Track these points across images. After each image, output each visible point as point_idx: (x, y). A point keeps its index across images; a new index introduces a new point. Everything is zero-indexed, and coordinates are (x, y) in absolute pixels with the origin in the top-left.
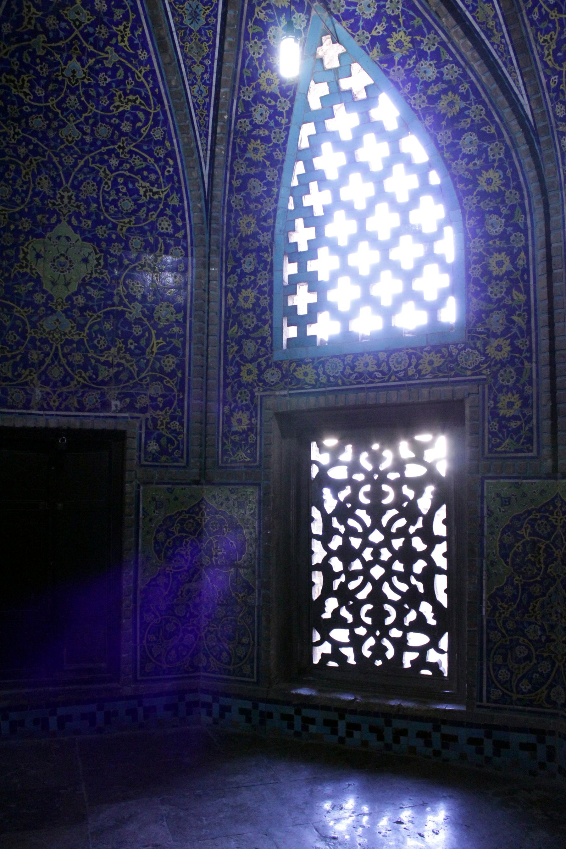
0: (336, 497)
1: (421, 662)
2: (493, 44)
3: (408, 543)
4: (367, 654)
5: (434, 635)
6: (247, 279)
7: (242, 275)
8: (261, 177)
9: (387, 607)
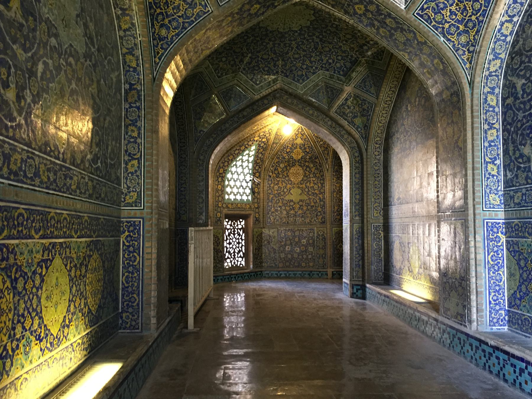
1: (240, 264)
4: (233, 264)
5: (242, 258)
7: (219, 182)
8: (228, 162)
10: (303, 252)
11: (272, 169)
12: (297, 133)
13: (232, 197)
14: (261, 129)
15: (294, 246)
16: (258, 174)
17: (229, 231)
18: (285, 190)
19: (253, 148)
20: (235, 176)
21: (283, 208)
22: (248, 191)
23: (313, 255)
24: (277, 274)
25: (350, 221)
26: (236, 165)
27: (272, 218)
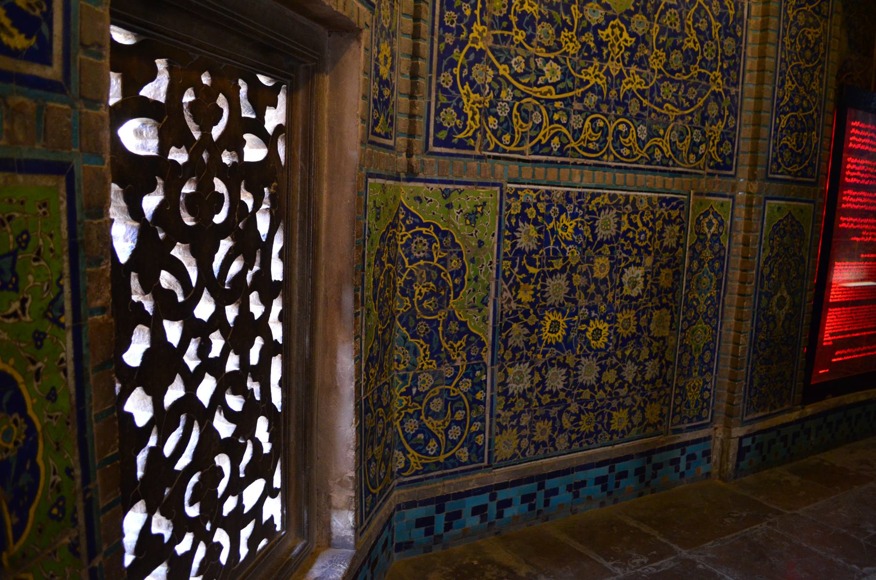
0: (135, 211)
10: (625, 341)
15: (583, 312)
21: (544, 30)
23: (668, 357)
24: (479, 510)
27: (470, 101)
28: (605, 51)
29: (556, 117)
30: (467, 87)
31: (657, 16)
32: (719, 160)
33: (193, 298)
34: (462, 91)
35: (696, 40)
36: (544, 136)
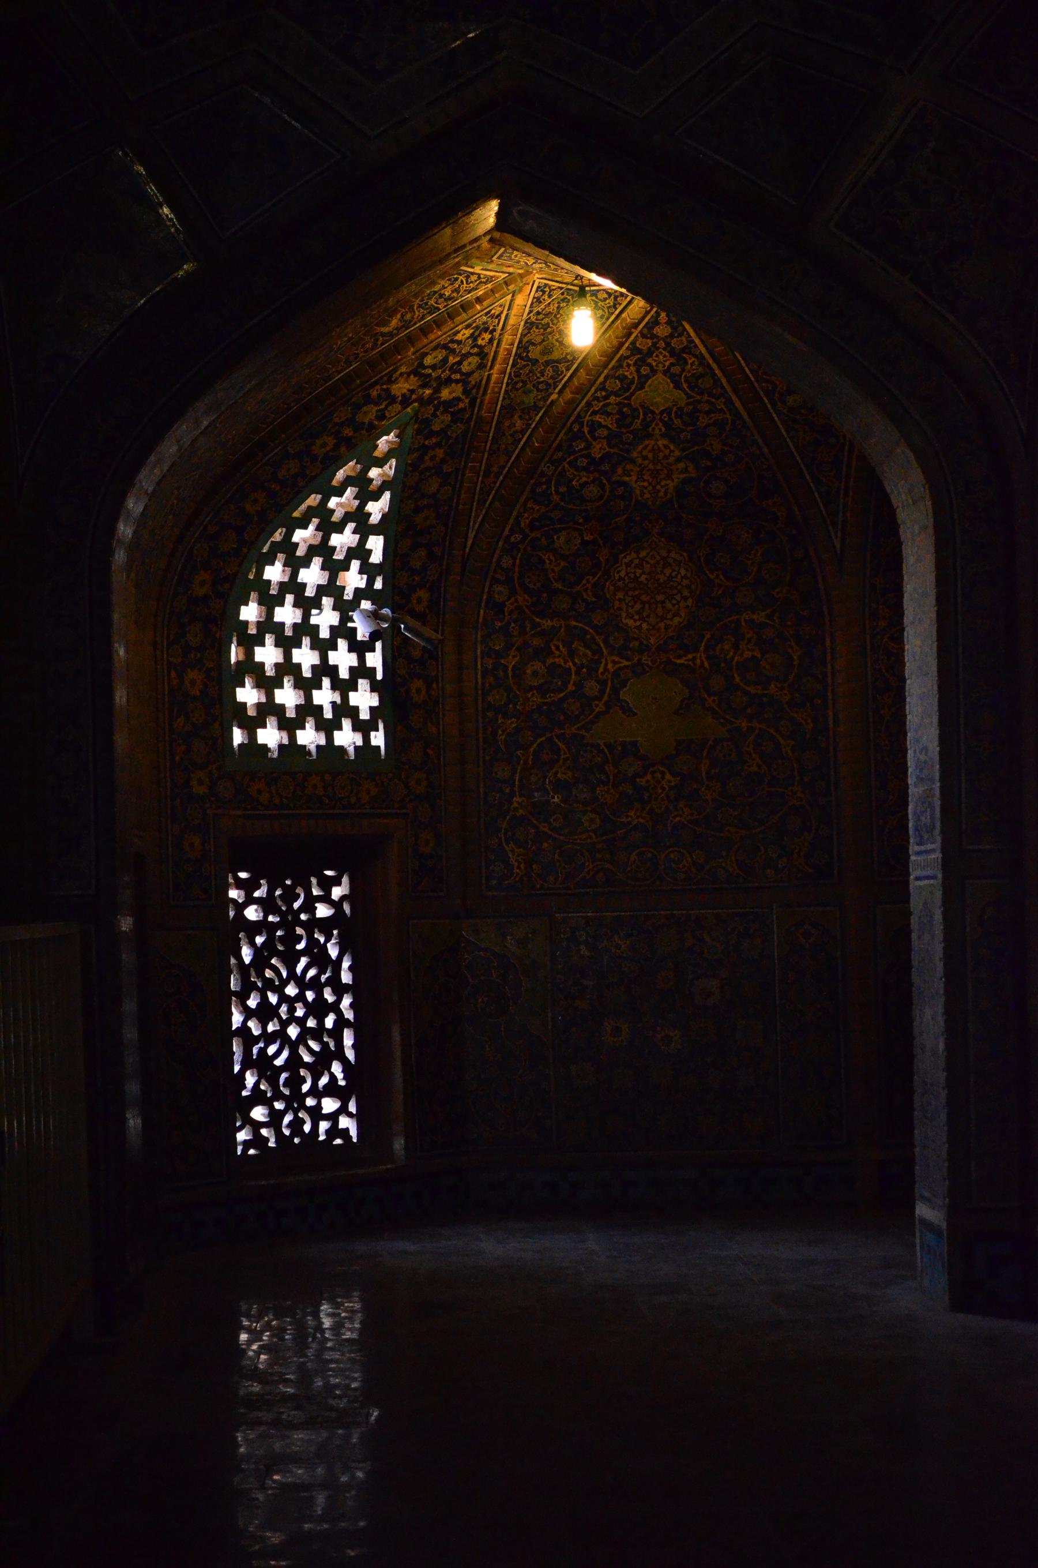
0: (252, 944)
1: (334, 1131)
2: (482, 482)
3: (319, 995)
6: (193, 655)
9: (303, 1072)
11: (506, 562)
12: (645, 344)
13: (270, 736)
14: (425, 331)
16: (423, 594)
17: (259, 940)
18: (591, 687)
19: (384, 443)
20: (287, 614)
22: (364, 699)
25: (946, 864)
26: (288, 547)
28: (646, 796)
29: (599, 856)
30: (511, 844)
31: (705, 753)
32: (810, 870)
33: (285, 983)
34: (507, 848)
35: (761, 763)
36: (588, 873)
